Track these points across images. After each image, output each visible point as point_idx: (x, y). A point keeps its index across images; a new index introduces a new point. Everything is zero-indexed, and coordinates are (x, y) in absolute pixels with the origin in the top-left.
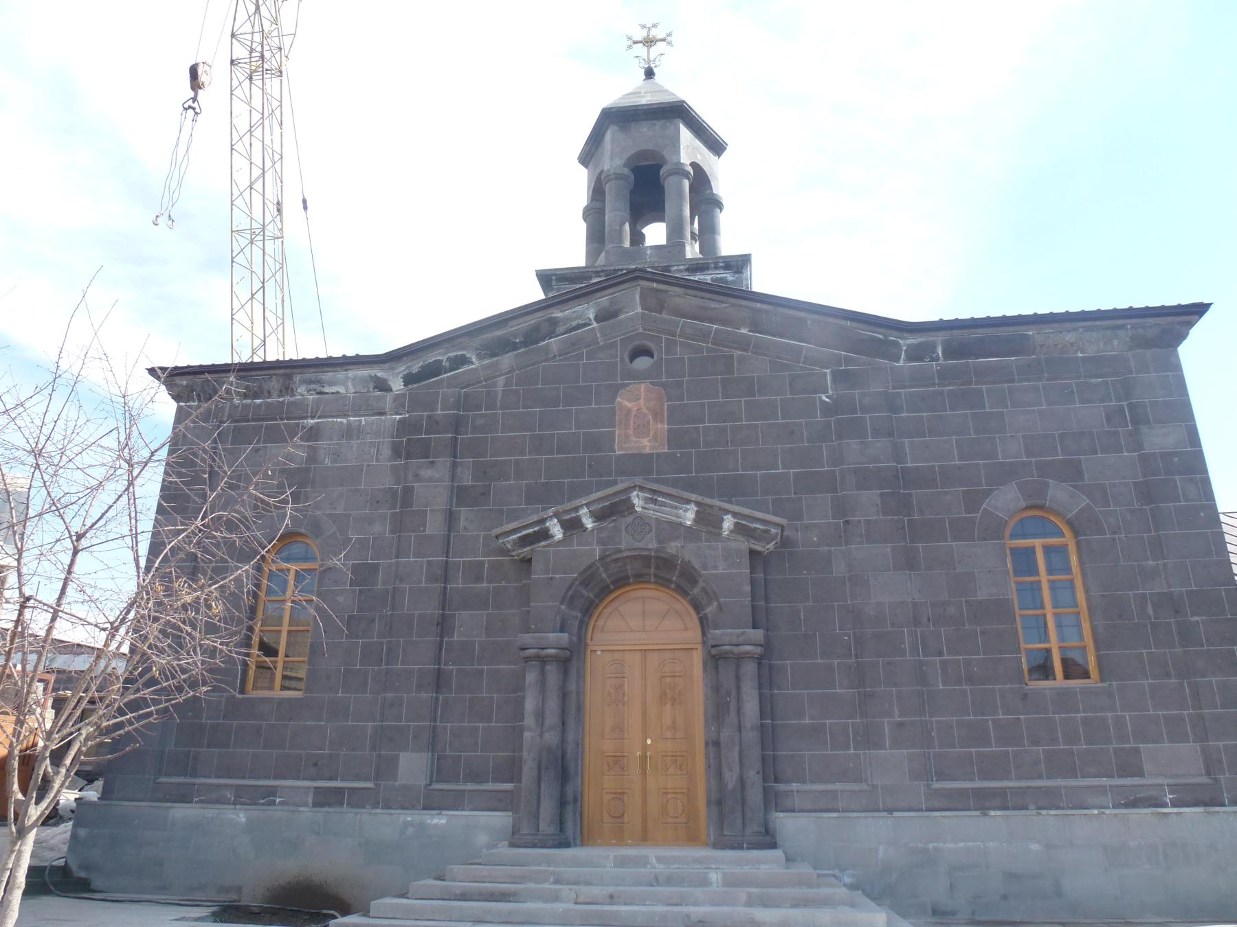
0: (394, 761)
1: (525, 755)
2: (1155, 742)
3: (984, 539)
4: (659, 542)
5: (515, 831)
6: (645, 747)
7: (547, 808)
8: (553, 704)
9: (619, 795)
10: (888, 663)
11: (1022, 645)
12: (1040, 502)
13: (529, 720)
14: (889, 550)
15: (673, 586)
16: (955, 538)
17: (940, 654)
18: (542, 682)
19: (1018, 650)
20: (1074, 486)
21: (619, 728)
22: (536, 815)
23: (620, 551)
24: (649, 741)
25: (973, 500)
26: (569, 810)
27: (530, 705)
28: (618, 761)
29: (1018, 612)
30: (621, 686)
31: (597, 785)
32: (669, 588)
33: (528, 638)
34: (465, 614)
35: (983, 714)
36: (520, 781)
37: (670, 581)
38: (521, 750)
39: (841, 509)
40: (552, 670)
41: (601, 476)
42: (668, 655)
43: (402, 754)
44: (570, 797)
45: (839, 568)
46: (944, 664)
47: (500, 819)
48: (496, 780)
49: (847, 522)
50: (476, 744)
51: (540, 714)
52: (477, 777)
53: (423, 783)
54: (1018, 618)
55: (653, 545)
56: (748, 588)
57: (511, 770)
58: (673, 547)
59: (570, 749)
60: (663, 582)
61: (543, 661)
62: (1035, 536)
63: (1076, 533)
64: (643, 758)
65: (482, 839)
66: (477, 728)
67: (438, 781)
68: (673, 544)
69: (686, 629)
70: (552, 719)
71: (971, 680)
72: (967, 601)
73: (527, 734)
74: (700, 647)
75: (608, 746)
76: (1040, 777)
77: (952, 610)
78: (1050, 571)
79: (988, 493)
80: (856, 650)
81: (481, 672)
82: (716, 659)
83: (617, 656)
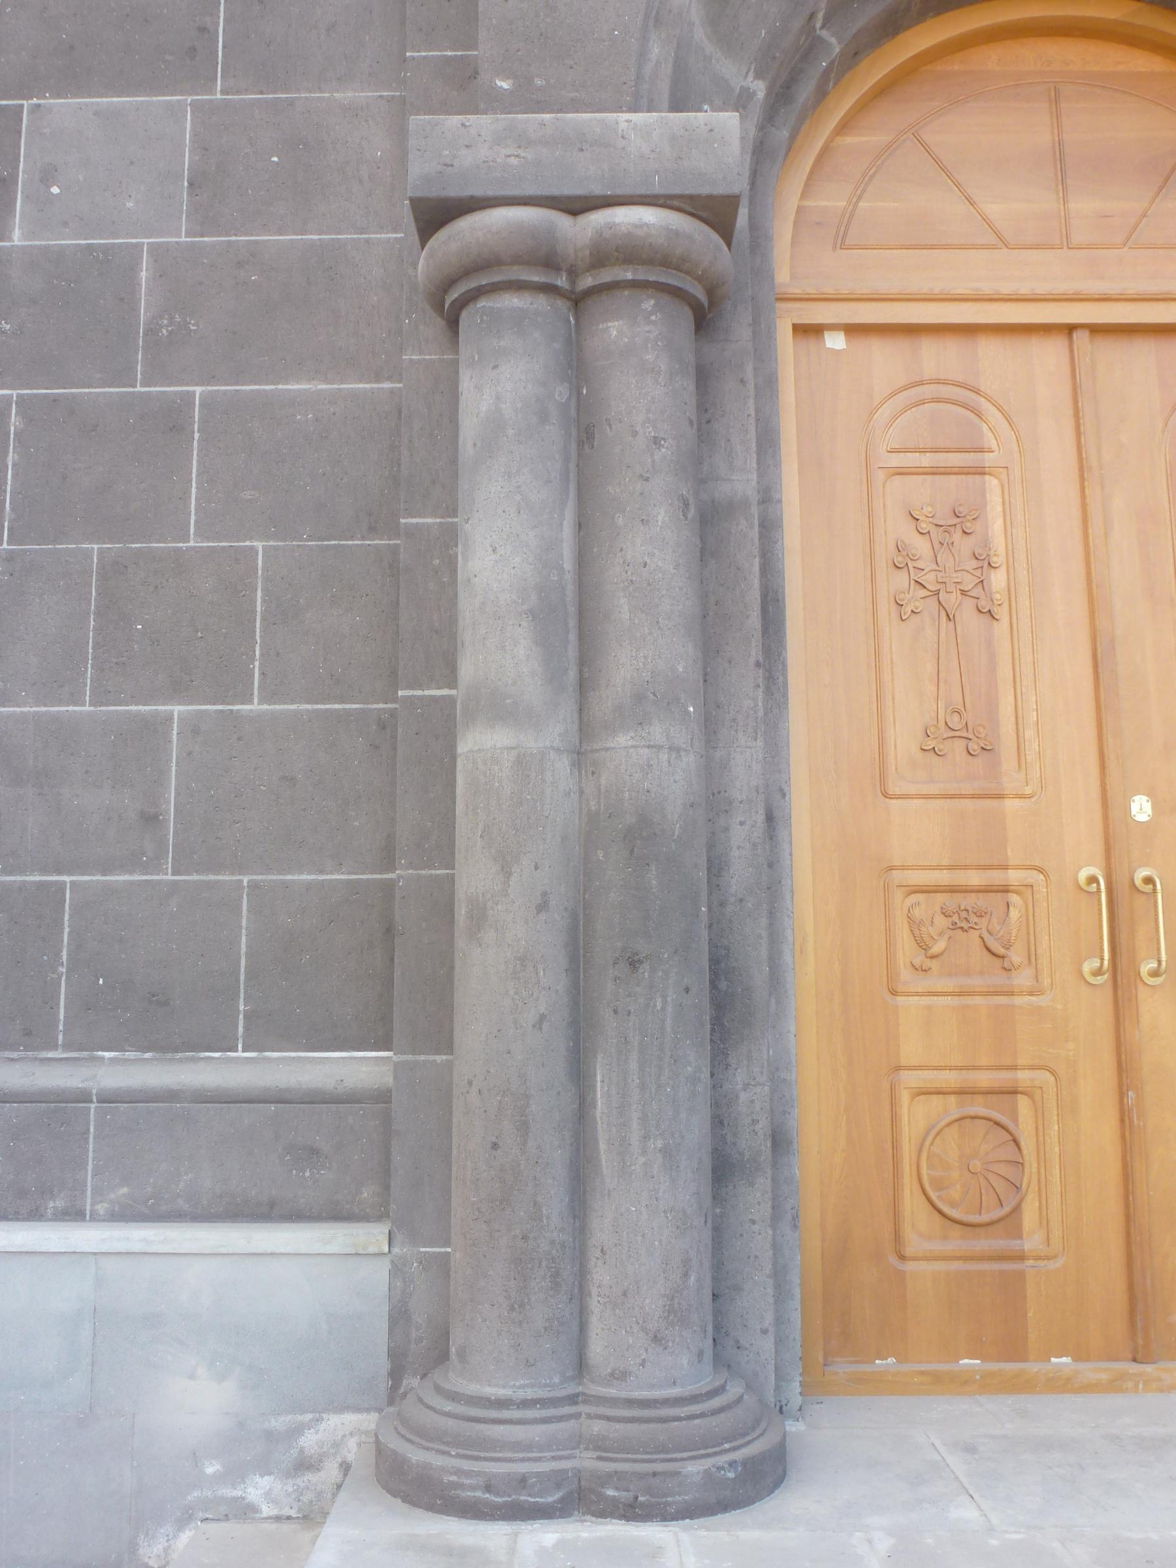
1: (474, 875)
5: (418, 1350)
6: (1113, 834)
7: (643, 1220)
8: (650, 546)
9: (991, 1105)
13: (499, 649)
18: (583, 431)
21: (968, 735)
22: (569, 1273)
24: (1141, 808)
26: (754, 1199)
27: (501, 549)
28: (974, 913)
30: (961, 520)
31: (859, 1037)
33: (469, 144)
34: (66, 109)
36: (439, 1034)
38: (440, 845)
40: (637, 342)
44: (752, 1139)
47: (315, 1274)
48: (275, 1030)
50: (151, 819)
51: (575, 622)
52: (156, 1015)
57: (386, 970)
59: (742, 832)
61: (578, 286)
64: (1122, 900)
65: (195, 1401)
66: (156, 728)
70: (648, 645)
73: (482, 744)
75: (918, 834)
81: (171, 420)
83: (936, 357)
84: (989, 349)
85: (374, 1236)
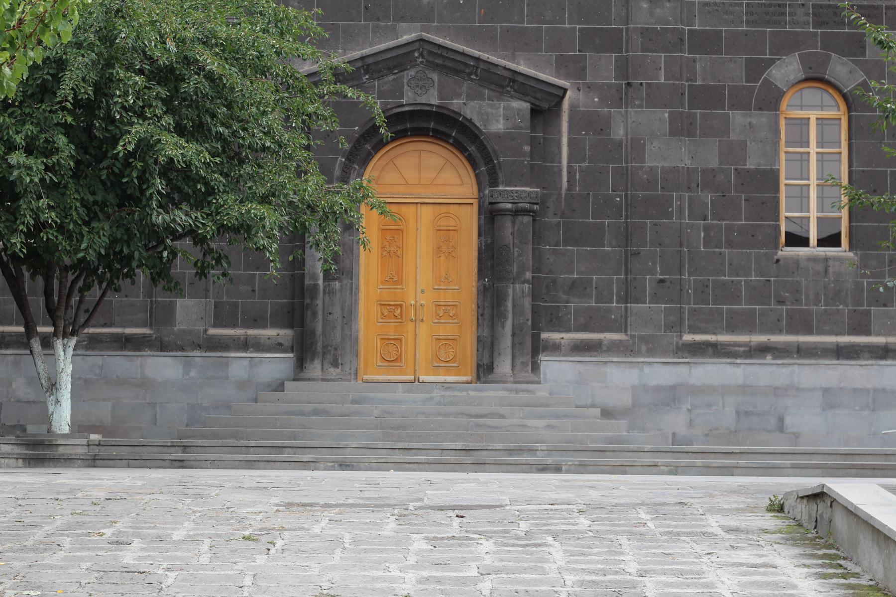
0: (171, 307)
2: (885, 305)
3: (760, 109)
4: (441, 98)
10: (656, 225)
11: (784, 213)
12: (819, 75)
14: (667, 115)
15: (451, 141)
16: (733, 107)
17: (705, 218)
19: (777, 218)
20: (853, 61)
23: (403, 106)
25: (755, 69)
29: (783, 181)
32: (447, 142)
35: (738, 275)
37: (450, 136)
39: (624, 69)
41: (378, 20)
42: (444, 209)
43: (179, 301)
45: (619, 132)
46: (707, 229)
49: (629, 84)
50: (254, 291)
52: (257, 321)
53: (202, 328)
54: (783, 188)
55: (435, 101)
56: (527, 148)
58: (456, 104)
60: (440, 136)
62: (812, 107)
63: (849, 109)
67: (215, 326)
68: (455, 101)
69: (462, 184)
71: (730, 244)
72: (736, 170)
74: (475, 202)
76: (780, 332)
77: (721, 177)
78: (820, 144)
79: (771, 62)
80: (626, 211)
82: (490, 216)
84: (403, 206)
85: (292, 355)
